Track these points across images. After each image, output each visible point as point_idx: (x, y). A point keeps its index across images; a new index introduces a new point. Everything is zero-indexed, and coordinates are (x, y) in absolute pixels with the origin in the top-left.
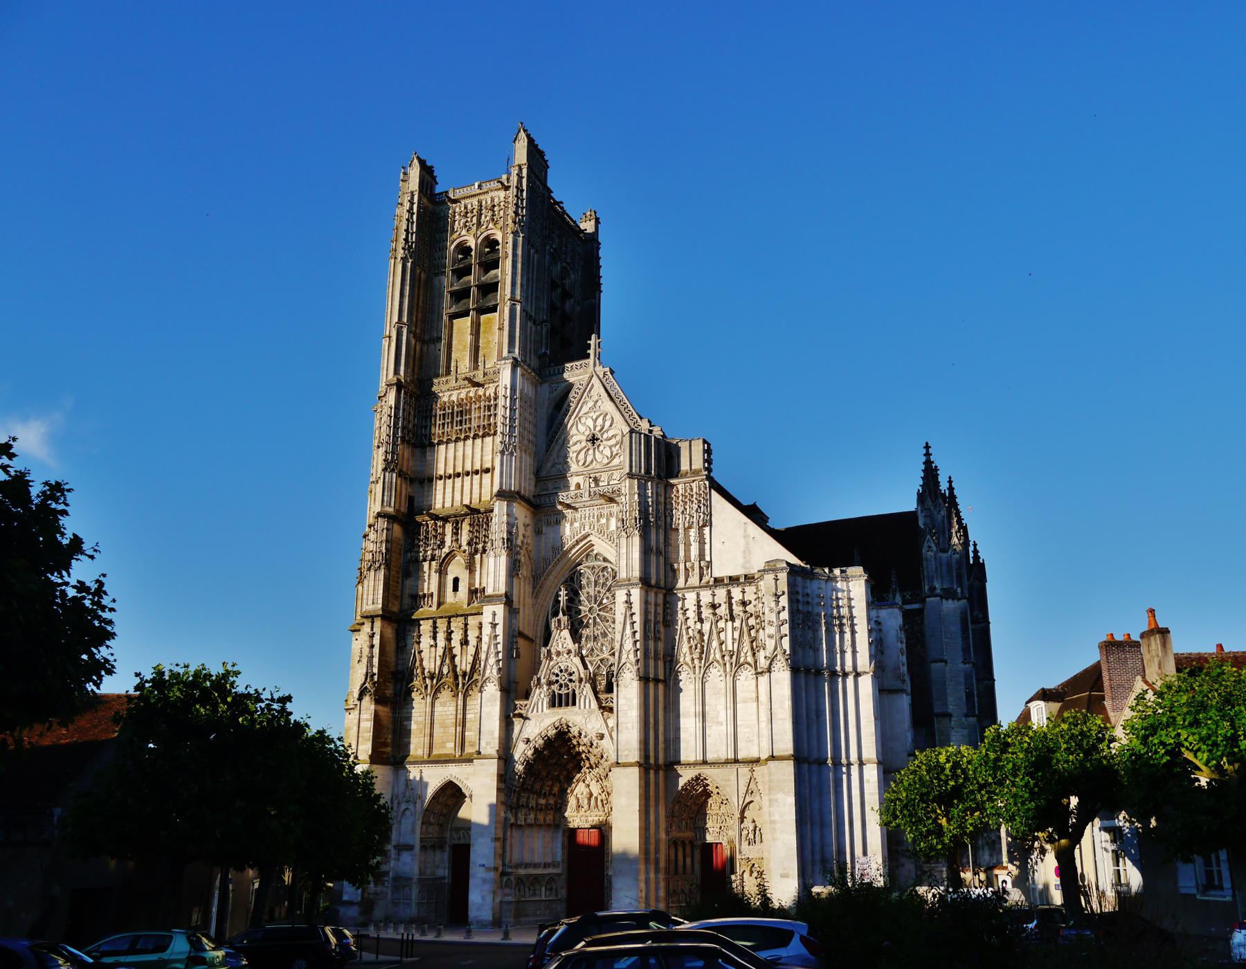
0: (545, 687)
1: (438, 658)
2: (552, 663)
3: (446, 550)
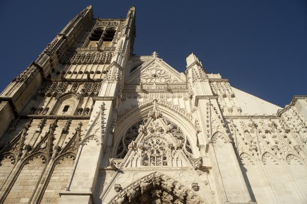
0: (140, 151)
1: (40, 137)
2: (145, 137)
3: (67, 92)
